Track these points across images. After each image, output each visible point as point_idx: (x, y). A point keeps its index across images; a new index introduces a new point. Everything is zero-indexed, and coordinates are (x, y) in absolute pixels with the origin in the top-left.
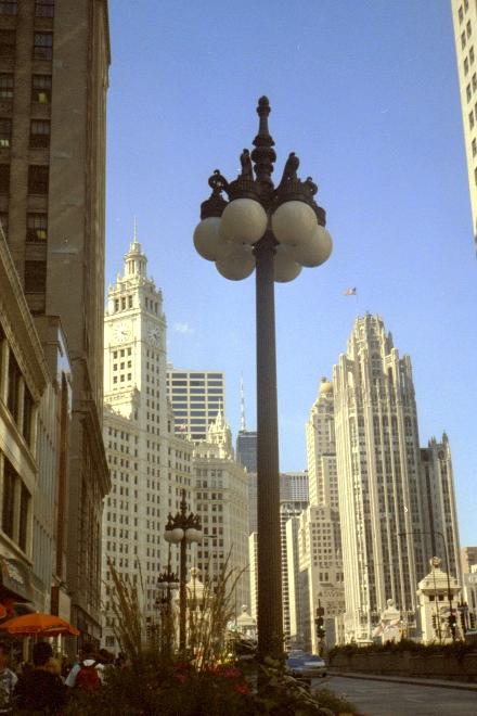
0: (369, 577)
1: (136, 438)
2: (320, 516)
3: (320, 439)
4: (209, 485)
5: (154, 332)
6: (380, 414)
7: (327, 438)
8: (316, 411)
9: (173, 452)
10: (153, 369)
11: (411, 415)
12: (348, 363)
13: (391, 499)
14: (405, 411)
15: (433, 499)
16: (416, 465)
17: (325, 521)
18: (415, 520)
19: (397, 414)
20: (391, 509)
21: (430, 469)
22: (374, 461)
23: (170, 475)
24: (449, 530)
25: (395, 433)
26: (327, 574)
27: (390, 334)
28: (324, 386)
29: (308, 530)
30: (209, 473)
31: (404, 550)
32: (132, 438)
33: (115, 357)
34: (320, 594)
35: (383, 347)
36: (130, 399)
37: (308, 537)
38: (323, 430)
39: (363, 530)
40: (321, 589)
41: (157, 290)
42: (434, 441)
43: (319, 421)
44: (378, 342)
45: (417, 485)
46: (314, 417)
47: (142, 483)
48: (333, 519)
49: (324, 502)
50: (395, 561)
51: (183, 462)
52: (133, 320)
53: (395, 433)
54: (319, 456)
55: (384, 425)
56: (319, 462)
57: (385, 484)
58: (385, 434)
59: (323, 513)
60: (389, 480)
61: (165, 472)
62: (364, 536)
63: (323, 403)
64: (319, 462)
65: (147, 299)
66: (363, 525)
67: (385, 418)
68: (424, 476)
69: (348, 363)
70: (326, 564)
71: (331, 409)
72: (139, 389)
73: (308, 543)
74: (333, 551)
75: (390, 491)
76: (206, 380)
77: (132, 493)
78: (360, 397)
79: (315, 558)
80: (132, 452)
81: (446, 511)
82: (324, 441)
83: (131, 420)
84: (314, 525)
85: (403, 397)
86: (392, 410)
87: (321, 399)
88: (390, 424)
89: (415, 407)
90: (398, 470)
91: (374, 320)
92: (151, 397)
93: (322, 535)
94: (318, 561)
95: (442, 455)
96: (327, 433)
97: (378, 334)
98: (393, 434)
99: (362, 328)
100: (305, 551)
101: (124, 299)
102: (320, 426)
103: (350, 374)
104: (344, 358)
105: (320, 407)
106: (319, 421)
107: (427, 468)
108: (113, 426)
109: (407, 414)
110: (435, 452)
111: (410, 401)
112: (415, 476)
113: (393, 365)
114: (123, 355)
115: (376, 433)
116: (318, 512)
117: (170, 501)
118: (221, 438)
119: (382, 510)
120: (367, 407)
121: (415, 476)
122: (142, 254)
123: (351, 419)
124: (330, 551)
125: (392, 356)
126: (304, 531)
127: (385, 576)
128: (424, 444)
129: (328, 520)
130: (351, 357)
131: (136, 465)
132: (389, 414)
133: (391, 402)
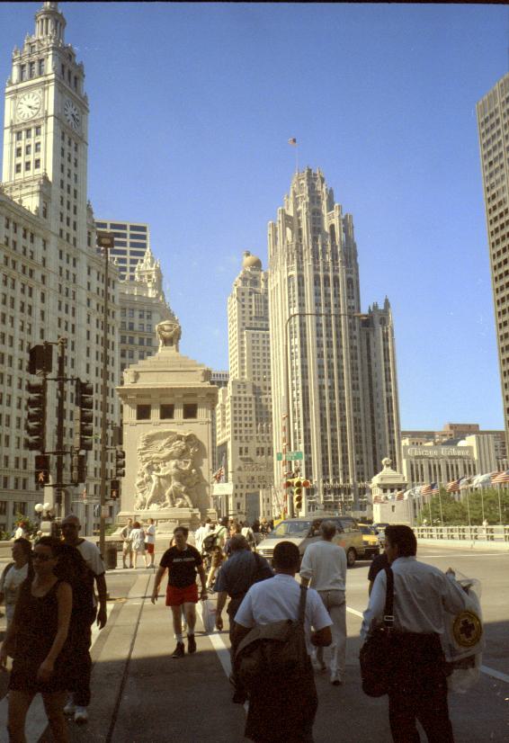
0: (305, 447)
1: (45, 242)
2: (242, 389)
3: (244, 312)
4: (136, 327)
5: (71, 110)
6: (321, 274)
7: (251, 313)
8: (240, 284)
10: (69, 191)
11: (353, 276)
12: (287, 218)
13: (330, 366)
14: (347, 272)
15: (373, 367)
16: (357, 330)
17: (247, 395)
18: (355, 387)
19: (340, 275)
20: (331, 376)
21: (371, 335)
22: (314, 324)
23: (89, 300)
24: (389, 400)
25: (336, 295)
26: (247, 449)
27: (331, 191)
28: (247, 260)
29: (228, 404)
30: (137, 314)
31: (343, 419)
32: (39, 242)
33: (19, 138)
34: (240, 469)
35: (324, 203)
37: (229, 410)
38: (246, 303)
39: (301, 397)
40: (241, 464)
41: (78, 61)
42: (375, 307)
43: (243, 294)
44: (319, 198)
45: (358, 352)
46: (238, 290)
47: (52, 302)
48: (254, 393)
49: (246, 377)
50: (334, 430)
52: (44, 89)
53: (336, 295)
54: (242, 330)
55: (325, 284)
56: (242, 336)
57: (325, 349)
58: (327, 295)
59: (245, 387)
60: (329, 345)
61: (82, 296)
62: (300, 402)
63: (248, 276)
64: (242, 336)
65: (63, 66)
66: (300, 392)
67: (326, 279)
68: (365, 342)
69: (287, 218)
70: (246, 438)
71: (255, 283)
72: (50, 179)
73: (229, 417)
74: (254, 425)
75: (330, 356)
76: (128, 232)
77: (37, 312)
78: (300, 253)
79: (236, 432)
80: (38, 259)
81: (386, 380)
82: (247, 315)
83: (38, 216)
84: (235, 399)
85: (346, 256)
86: (334, 270)
87: (245, 272)
88: (331, 284)
89: (357, 269)
90: (339, 335)
91: (315, 175)
92: (66, 194)
93: (243, 409)
94: (238, 434)
95: (384, 321)
96: (251, 306)
97: (319, 188)
98: (335, 296)
99: (302, 182)
100: (224, 425)
101: (31, 64)
102: (243, 300)
103: (288, 229)
104: (283, 211)
105: (244, 280)
106: (243, 294)
107: (368, 334)
108: (12, 216)
109: (349, 275)
110: (377, 319)
111: (353, 262)
112: (356, 343)
113: (336, 222)
114: (28, 136)
115: (317, 294)
116: (239, 385)
117: (88, 366)
118: (150, 277)
119: (321, 377)
120: (308, 264)
121: (356, 343)
122: (60, 12)
123: (290, 278)
124: (251, 425)
125: (336, 212)
126: (223, 407)
127: (322, 446)
128: (364, 311)
129: (249, 394)
130: (291, 213)
131: (43, 278)
132: (331, 274)
133: (332, 261)
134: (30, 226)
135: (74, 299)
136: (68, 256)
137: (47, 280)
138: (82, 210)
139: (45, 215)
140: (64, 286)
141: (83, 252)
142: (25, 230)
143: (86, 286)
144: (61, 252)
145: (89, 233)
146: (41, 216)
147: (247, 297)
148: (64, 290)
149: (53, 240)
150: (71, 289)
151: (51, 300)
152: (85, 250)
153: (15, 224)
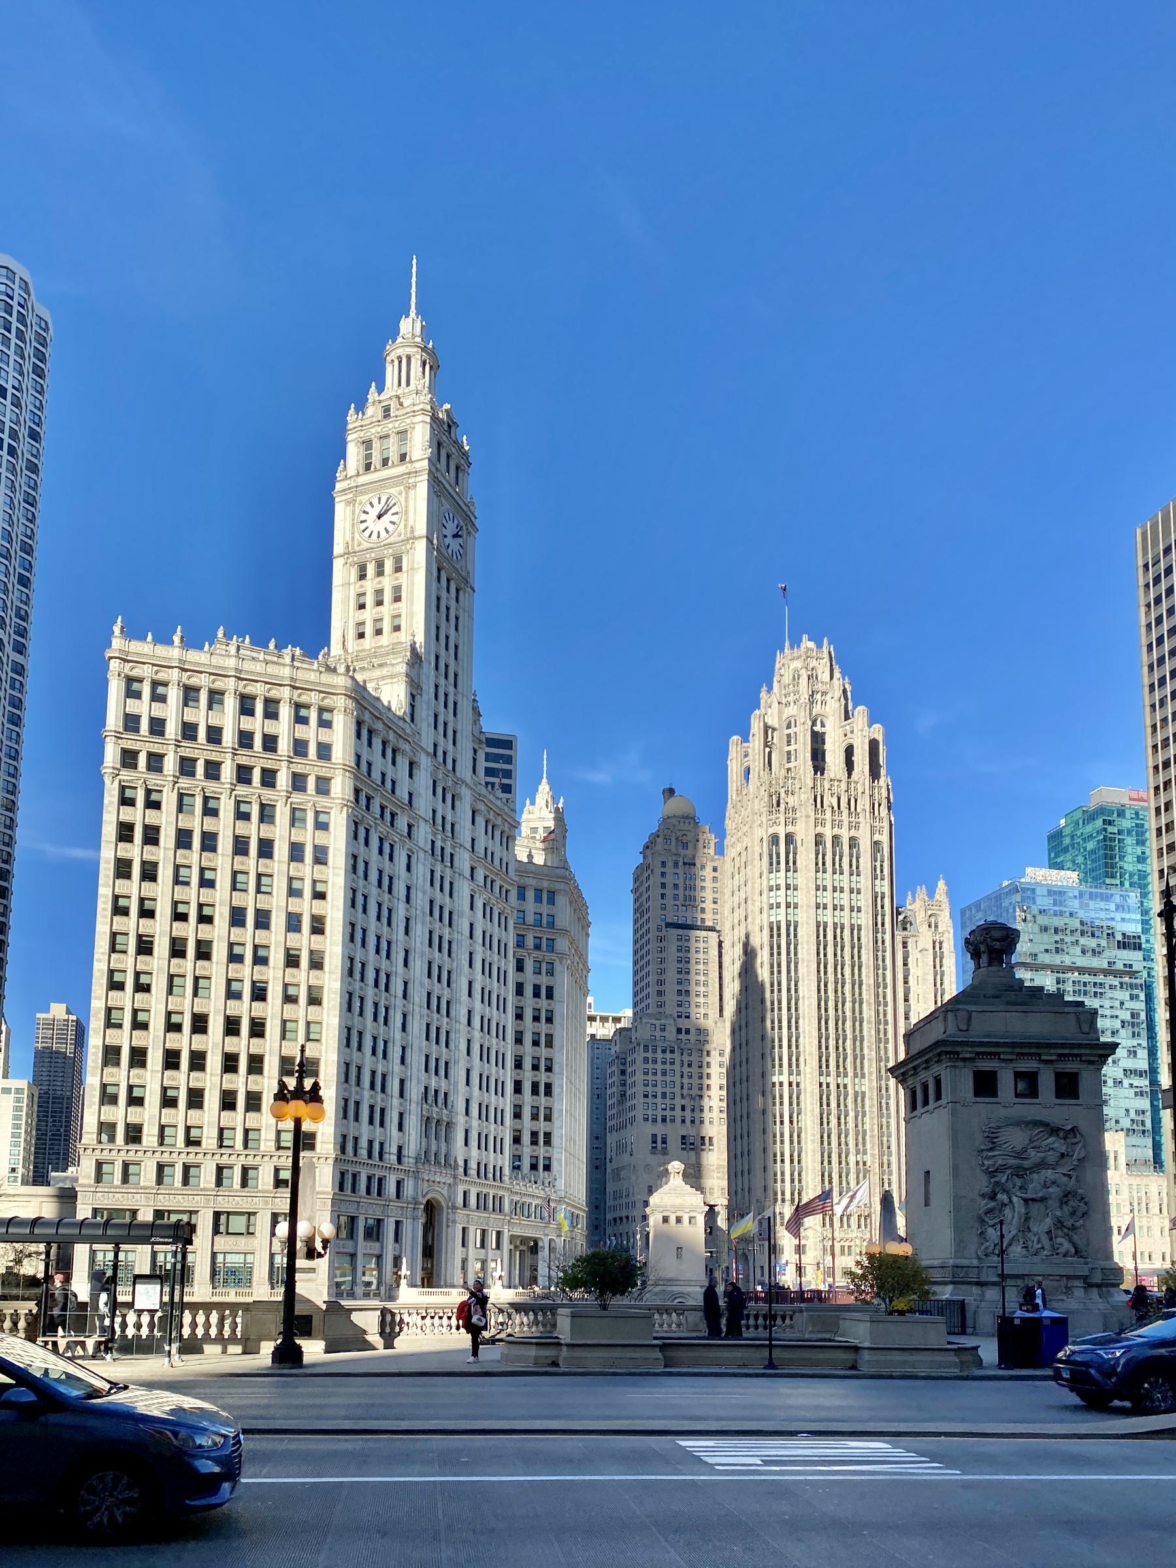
6: (828, 833)
9: (480, 821)
30: (530, 895)
32: (403, 763)
36: (402, 668)
47: (421, 870)
51: (499, 852)
61: (464, 861)
80: (403, 793)
134: (391, 736)
135: (452, 866)
136: (444, 789)
137: (414, 830)
138: (465, 708)
139: (412, 715)
140: (438, 844)
141: (467, 785)
142: (384, 743)
143: (468, 845)
144: (434, 782)
145: (475, 751)
146: (408, 719)
147: (669, 869)
148: (438, 851)
149: (424, 761)
150: (448, 851)
151: (421, 867)
152: (469, 780)
153: (370, 732)
